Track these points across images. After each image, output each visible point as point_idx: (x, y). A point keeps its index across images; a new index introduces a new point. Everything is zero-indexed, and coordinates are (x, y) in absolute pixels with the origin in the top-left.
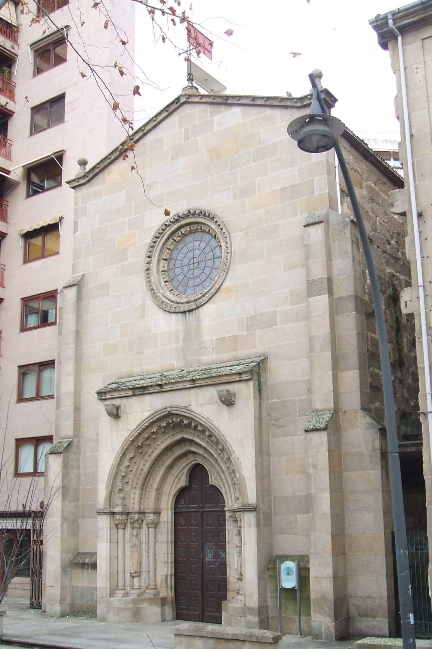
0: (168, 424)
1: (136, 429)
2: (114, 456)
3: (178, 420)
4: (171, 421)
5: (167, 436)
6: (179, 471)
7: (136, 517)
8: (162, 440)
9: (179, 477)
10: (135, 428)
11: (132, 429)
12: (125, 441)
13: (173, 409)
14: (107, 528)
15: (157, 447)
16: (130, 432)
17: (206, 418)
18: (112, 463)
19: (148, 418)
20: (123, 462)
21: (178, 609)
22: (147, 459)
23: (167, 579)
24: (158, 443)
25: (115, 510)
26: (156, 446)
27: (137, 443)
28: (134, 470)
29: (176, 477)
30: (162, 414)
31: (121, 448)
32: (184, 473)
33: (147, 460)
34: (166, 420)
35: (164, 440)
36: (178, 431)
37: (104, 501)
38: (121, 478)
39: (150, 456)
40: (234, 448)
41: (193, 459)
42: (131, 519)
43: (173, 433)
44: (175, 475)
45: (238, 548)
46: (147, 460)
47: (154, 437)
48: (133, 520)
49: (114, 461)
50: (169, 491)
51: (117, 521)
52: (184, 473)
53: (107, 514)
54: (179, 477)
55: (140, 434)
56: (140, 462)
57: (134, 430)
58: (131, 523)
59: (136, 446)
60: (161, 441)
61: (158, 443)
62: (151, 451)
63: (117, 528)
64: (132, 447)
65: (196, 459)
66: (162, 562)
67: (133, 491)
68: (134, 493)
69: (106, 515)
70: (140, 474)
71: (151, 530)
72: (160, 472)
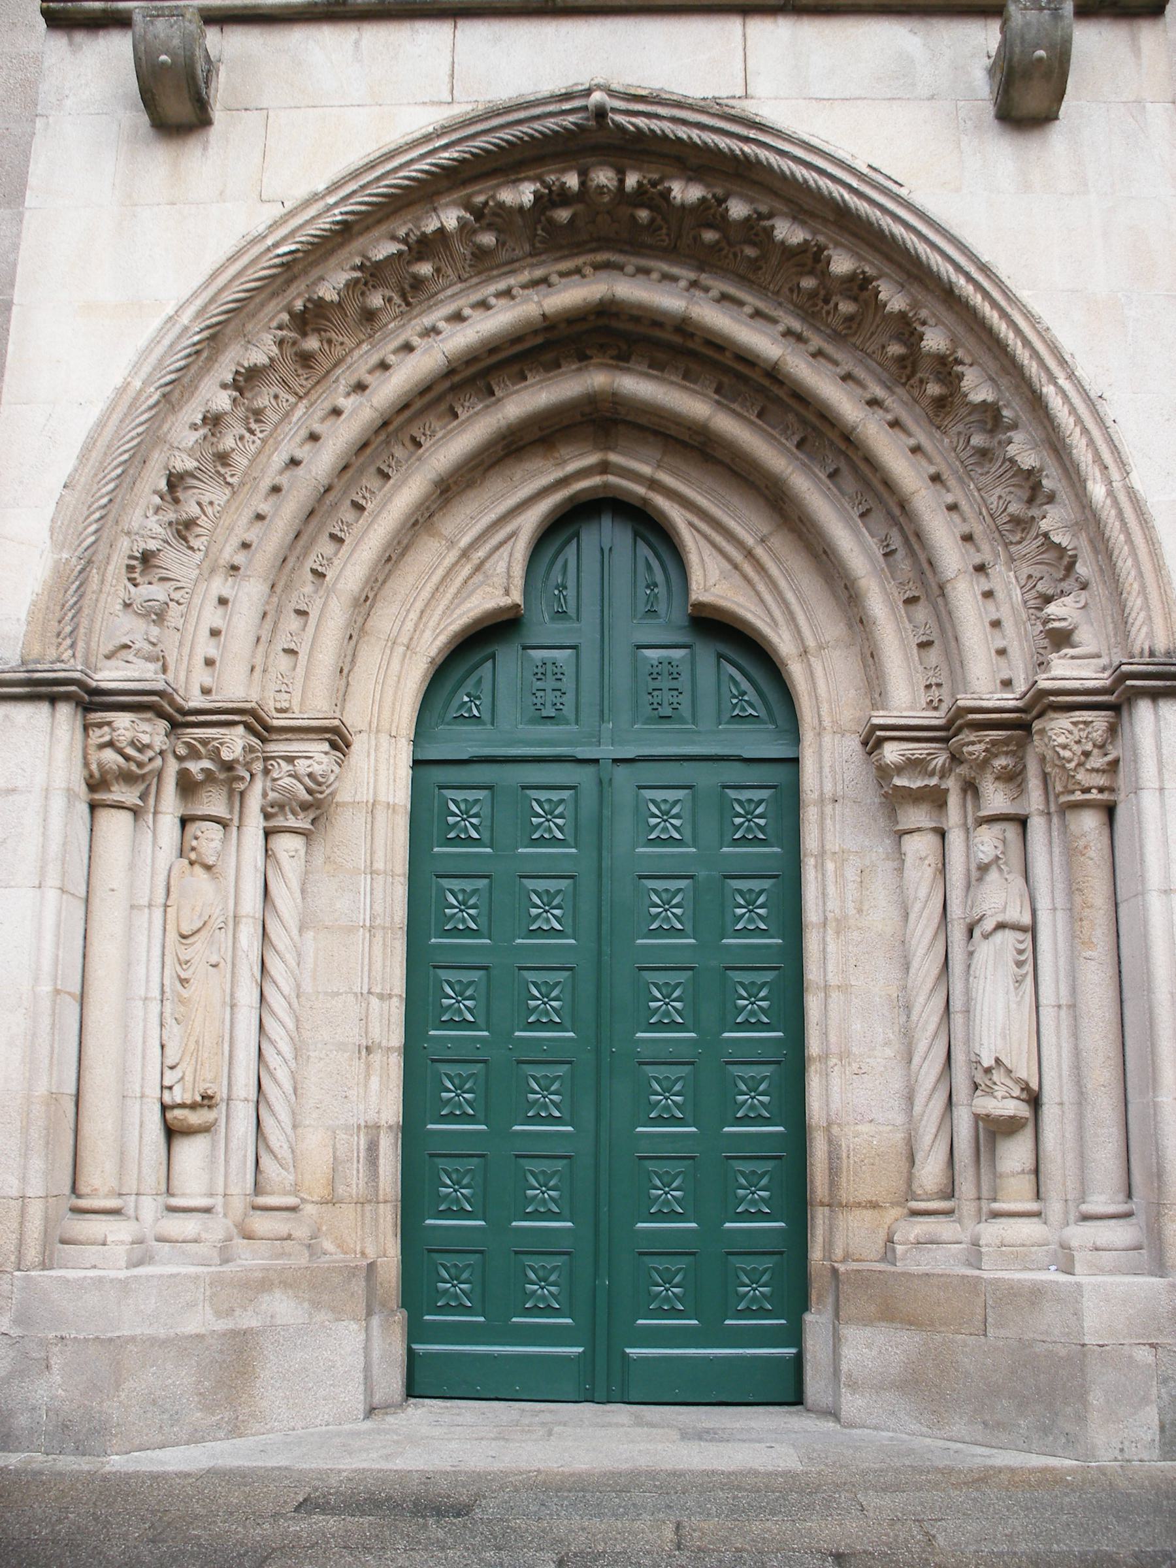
0: (548, 200)
1: (330, 190)
2: (142, 342)
3: (631, 180)
4: (572, 181)
5: (502, 285)
6: (492, 516)
7: (234, 742)
8: (462, 303)
9: (481, 554)
10: (321, 187)
11: (301, 192)
12: (232, 259)
13: (621, 105)
14: (47, 792)
15: (416, 341)
16: (277, 211)
17: (865, 170)
18: (118, 381)
19: (427, 138)
20: (193, 386)
21: (415, 1331)
22: (342, 402)
23: (373, 1148)
24: (427, 320)
25: (110, 676)
26: (410, 333)
27: (315, 283)
28: (241, 461)
29: (465, 554)
30: (537, 125)
31: (195, 295)
32: (513, 535)
33: (336, 412)
34: (539, 178)
35: (499, 295)
36: (579, 261)
37: (31, 613)
38: (163, 485)
39: (360, 387)
40: (1067, 342)
41: (592, 459)
42: (194, 754)
43: (539, 273)
44: (464, 542)
45: (1000, 936)
46: (336, 412)
47: (425, 269)
48: (206, 764)
49: (136, 367)
50: (409, 625)
51: (109, 756)
52: (513, 535)
53: (53, 700)
54: (481, 554)
55: (346, 231)
56: (287, 415)
57: (315, 197)
58: (187, 786)
59: (299, 305)
60: (449, 309)
61: (427, 320)
62: (374, 359)
63: (93, 807)
64: (272, 307)
65: (613, 458)
66: (341, 1047)
67: (219, 585)
68: (223, 601)
69: (44, 708)
70: (276, 489)
71: (286, 845)
72: (383, 505)
